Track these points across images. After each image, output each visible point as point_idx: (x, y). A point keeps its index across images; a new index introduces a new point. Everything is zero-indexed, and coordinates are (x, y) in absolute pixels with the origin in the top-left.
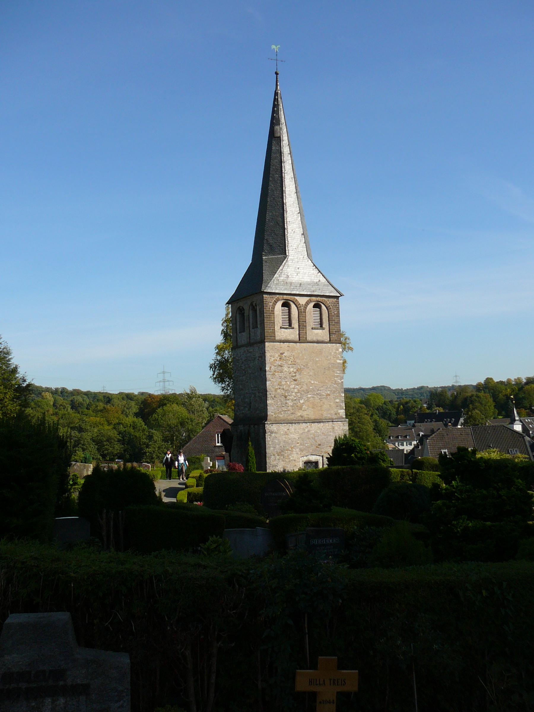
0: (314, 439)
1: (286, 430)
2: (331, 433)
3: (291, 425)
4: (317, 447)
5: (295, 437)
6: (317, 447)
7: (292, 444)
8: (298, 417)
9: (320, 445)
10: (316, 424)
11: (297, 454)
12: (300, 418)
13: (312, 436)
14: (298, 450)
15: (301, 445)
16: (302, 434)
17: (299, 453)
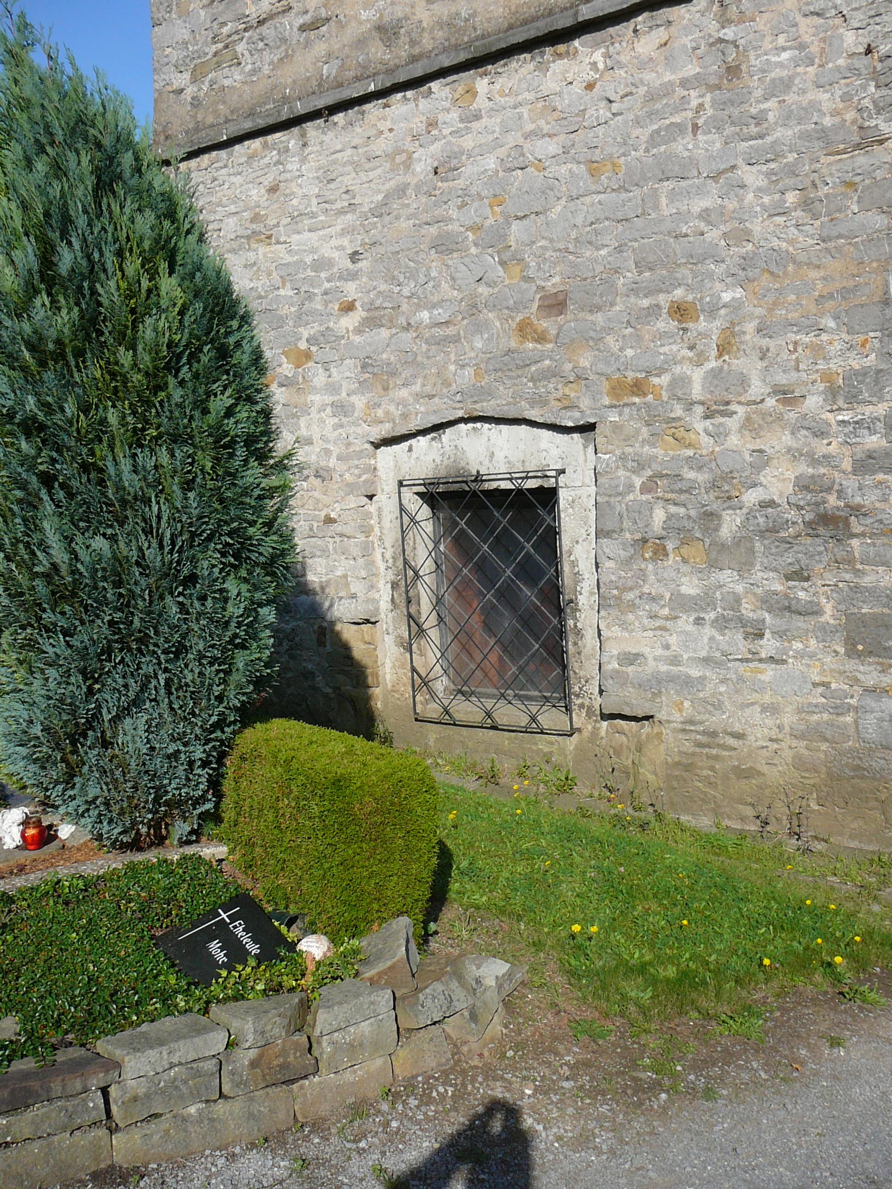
0: (496, 241)
1: (257, 194)
2: (709, 143)
3: (288, 139)
4: (524, 329)
5: (327, 251)
6: (524, 329)
7: (300, 319)
8: (361, 42)
9: (555, 304)
10: (519, 72)
11: (341, 409)
12: (378, 52)
13: (471, 215)
14: (346, 372)
15: (371, 322)
16: (378, 212)
17: (359, 402)
